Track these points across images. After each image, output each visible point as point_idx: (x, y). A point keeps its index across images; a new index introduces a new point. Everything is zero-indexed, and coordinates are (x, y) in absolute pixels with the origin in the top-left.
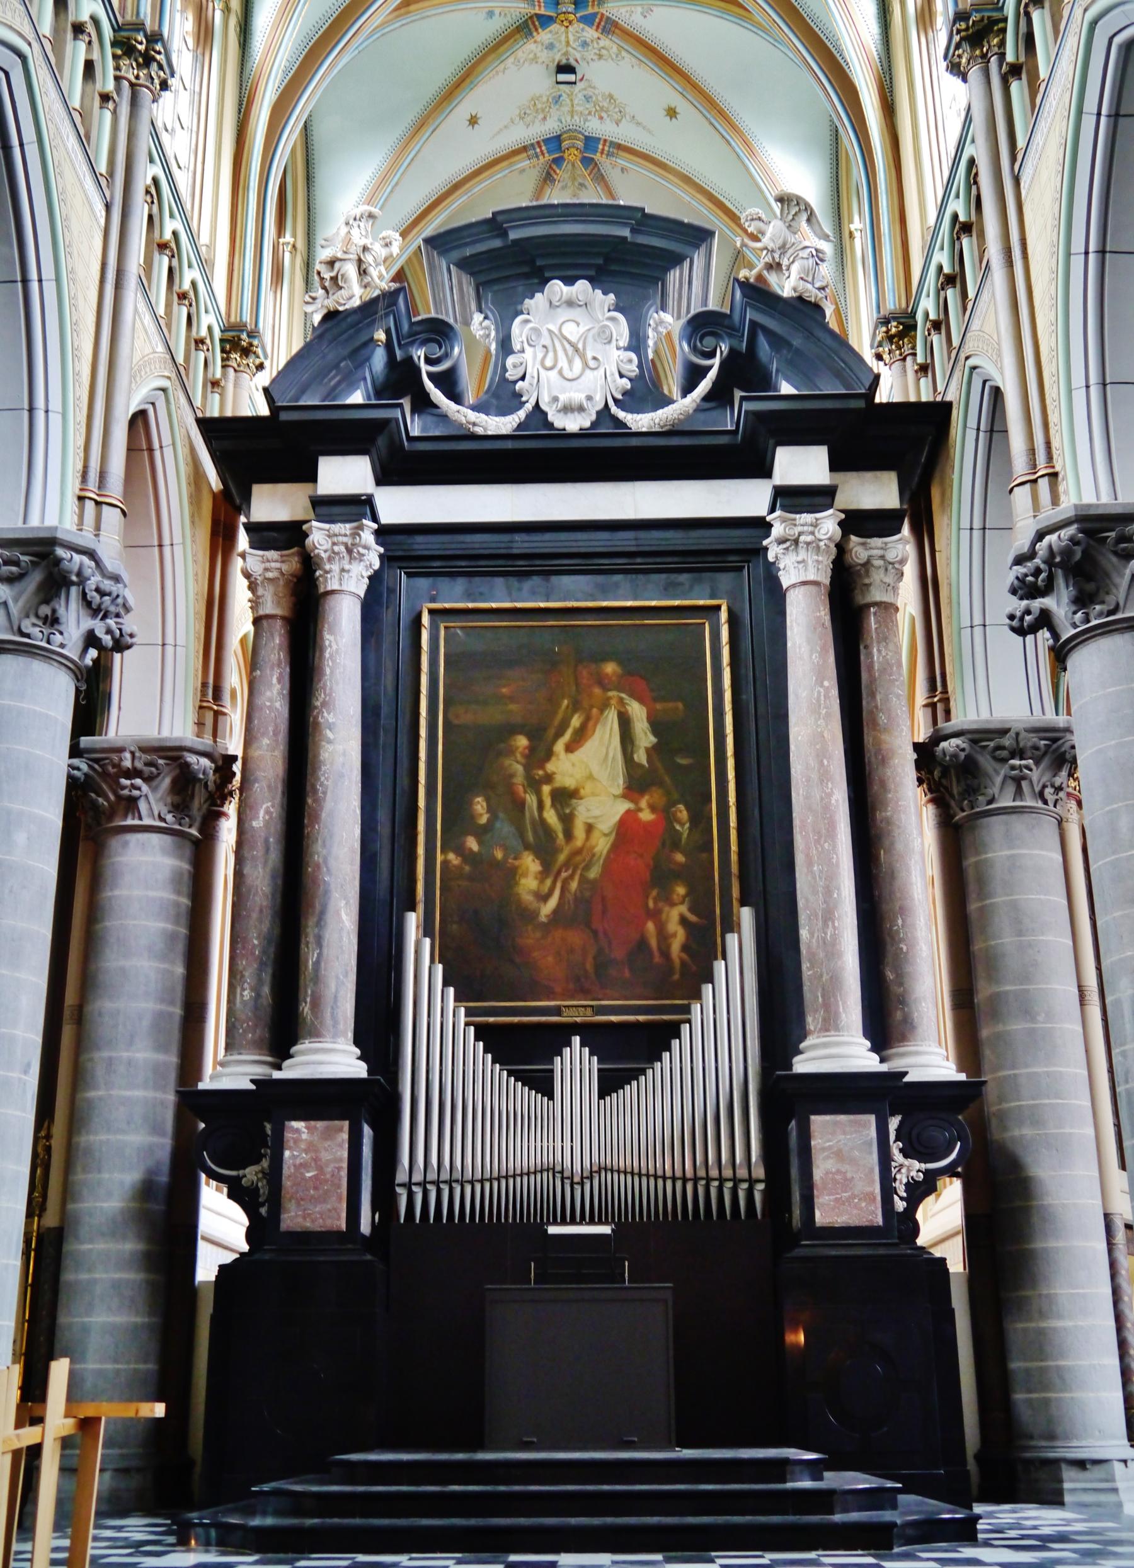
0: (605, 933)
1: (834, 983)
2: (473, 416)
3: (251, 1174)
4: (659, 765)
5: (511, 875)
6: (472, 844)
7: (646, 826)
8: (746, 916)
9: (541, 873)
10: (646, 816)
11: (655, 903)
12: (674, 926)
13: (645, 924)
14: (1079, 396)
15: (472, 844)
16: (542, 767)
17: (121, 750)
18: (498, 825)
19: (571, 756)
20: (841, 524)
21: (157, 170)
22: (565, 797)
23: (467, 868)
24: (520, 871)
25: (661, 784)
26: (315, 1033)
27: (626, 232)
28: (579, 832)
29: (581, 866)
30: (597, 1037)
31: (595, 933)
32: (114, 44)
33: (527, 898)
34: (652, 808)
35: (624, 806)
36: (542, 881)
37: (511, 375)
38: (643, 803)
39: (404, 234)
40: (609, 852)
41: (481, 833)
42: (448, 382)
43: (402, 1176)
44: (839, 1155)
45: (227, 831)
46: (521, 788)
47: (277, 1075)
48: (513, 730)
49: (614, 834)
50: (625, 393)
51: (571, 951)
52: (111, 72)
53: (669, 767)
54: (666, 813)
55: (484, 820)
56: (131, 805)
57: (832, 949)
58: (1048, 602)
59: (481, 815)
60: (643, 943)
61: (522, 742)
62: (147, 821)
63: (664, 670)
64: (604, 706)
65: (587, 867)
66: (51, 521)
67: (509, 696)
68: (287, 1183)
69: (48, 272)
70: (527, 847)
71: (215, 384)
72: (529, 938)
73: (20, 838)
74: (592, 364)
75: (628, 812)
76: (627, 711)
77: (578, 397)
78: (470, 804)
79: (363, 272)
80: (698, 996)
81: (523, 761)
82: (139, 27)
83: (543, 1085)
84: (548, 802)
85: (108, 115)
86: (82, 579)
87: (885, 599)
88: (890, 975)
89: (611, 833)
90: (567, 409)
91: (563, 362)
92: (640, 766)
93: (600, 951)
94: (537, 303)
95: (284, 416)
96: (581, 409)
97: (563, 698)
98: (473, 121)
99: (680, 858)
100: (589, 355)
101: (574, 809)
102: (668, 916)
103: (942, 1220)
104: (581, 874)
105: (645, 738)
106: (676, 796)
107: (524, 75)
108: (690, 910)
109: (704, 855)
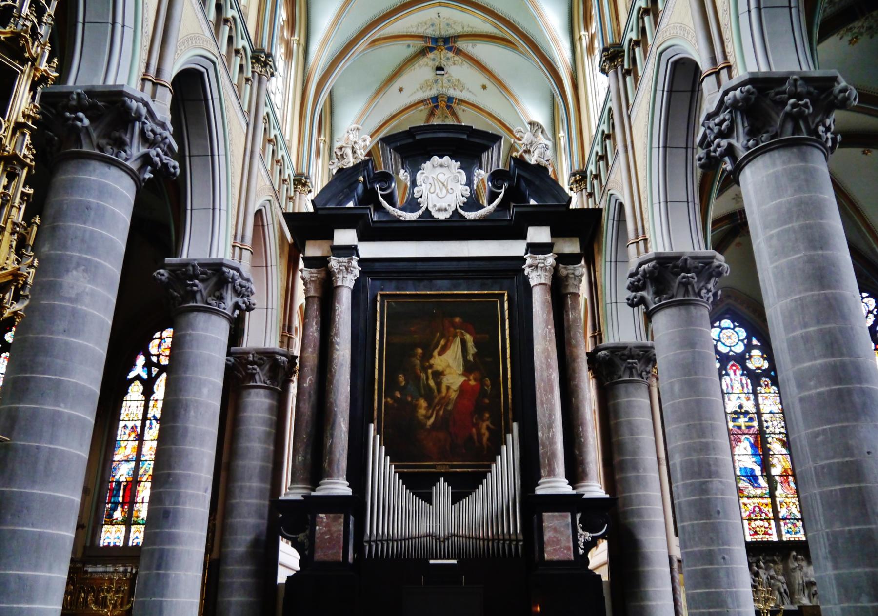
1: (553, 456)
2: (400, 212)
3: (301, 537)
5: (415, 407)
6: (398, 395)
8: (515, 426)
10: (472, 383)
12: (484, 430)
14: (656, 207)
15: (398, 395)
17: (248, 353)
19: (441, 357)
20: (555, 259)
21: (268, 109)
22: (438, 375)
23: (396, 405)
26: (330, 476)
27: (465, 137)
30: (451, 479)
32: (252, 58)
33: (421, 418)
34: (475, 380)
37: (416, 195)
38: (471, 377)
39: (371, 136)
41: (402, 390)
42: (390, 199)
43: (367, 538)
44: (555, 530)
45: (293, 388)
47: (313, 493)
50: (464, 203)
52: (250, 69)
53: (481, 363)
54: (480, 381)
55: (403, 384)
56: (252, 377)
57: (552, 441)
58: (644, 293)
60: (471, 437)
61: (420, 351)
62: (259, 384)
63: (481, 320)
64: (455, 336)
65: (447, 405)
66: (221, 256)
68: (317, 541)
69: (222, 152)
70: (421, 396)
71: (291, 198)
73: (205, 391)
74: (450, 191)
77: (444, 205)
78: (397, 377)
79: (354, 152)
80: (495, 461)
82: (262, 51)
83: (427, 498)
84: (430, 377)
85: (248, 87)
86: (234, 280)
87: (574, 291)
88: (577, 452)
90: (440, 210)
91: (438, 190)
92: (470, 361)
94: (427, 165)
95: (320, 212)
96: (446, 210)
98: (401, 90)
99: (487, 401)
100: (449, 188)
103: (599, 557)
105: (472, 349)
107: (423, 71)
108: (492, 423)
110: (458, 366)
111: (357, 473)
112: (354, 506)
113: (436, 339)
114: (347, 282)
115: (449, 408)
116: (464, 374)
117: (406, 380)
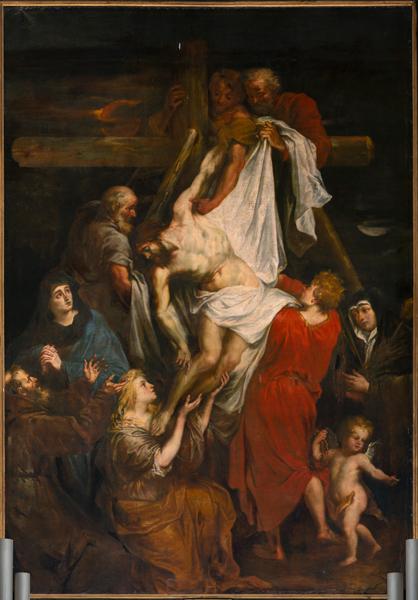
0: (250, 498)
4: (332, 235)
5: (112, 405)
6: (52, 357)
7: (313, 332)
9: (154, 402)
10: (313, 317)
11: (323, 450)
13: (309, 480)
16: (156, 239)
18: (90, 329)
19: (202, 220)
22: (191, 287)
23: (45, 394)
24: (124, 401)
25: (335, 268)
28: (212, 342)
29: (214, 394)
31: (234, 494)
34: (322, 305)
35: (279, 301)
36: (156, 416)
38: (309, 297)
40: (255, 372)
41: (66, 340)
46: (124, 269)
48: (107, 178)
49: (264, 345)
51: (200, 518)
54: (341, 311)
55: (69, 320)
59: (66, 312)
61: (126, 197)
64: (253, 140)
65: (223, 396)
67: (105, 128)
70: (133, 366)
72: (137, 499)
75: (285, 309)
76: (287, 149)
78: (49, 294)
81: (128, 228)
84: (164, 295)
89: (259, 342)
92: (305, 237)
93: (242, 520)
97: (190, 127)
99: (361, 382)
101: (205, 306)
102: (341, 471)
104: (214, 406)
105: (313, 194)
106: (359, 287)
108: (374, 462)
109: (398, 379)
110: (264, 258)
113: (184, 155)
115: (232, 405)
116: (281, 286)
117: (77, 304)
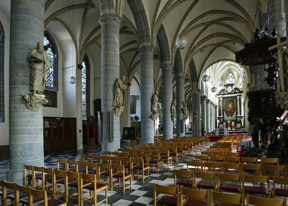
53: (233, 105)
63: (233, 102)
111: (223, 115)
112: (223, 118)
114: (221, 100)
